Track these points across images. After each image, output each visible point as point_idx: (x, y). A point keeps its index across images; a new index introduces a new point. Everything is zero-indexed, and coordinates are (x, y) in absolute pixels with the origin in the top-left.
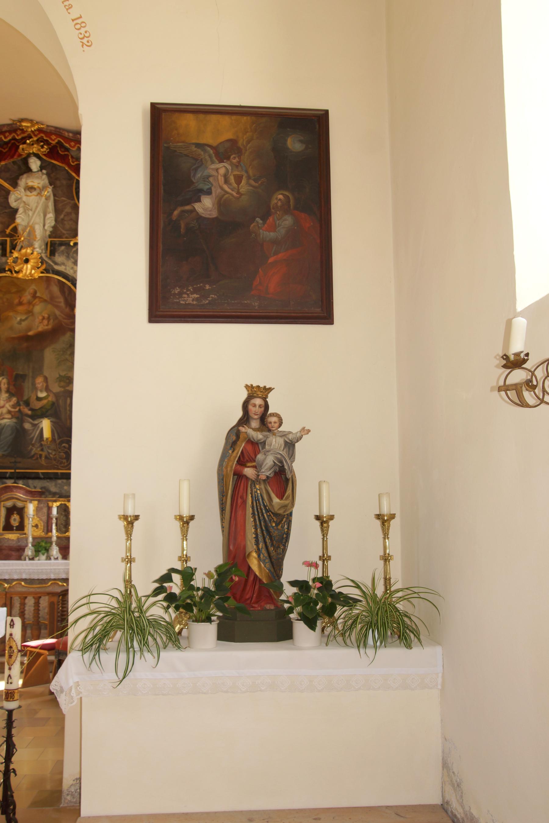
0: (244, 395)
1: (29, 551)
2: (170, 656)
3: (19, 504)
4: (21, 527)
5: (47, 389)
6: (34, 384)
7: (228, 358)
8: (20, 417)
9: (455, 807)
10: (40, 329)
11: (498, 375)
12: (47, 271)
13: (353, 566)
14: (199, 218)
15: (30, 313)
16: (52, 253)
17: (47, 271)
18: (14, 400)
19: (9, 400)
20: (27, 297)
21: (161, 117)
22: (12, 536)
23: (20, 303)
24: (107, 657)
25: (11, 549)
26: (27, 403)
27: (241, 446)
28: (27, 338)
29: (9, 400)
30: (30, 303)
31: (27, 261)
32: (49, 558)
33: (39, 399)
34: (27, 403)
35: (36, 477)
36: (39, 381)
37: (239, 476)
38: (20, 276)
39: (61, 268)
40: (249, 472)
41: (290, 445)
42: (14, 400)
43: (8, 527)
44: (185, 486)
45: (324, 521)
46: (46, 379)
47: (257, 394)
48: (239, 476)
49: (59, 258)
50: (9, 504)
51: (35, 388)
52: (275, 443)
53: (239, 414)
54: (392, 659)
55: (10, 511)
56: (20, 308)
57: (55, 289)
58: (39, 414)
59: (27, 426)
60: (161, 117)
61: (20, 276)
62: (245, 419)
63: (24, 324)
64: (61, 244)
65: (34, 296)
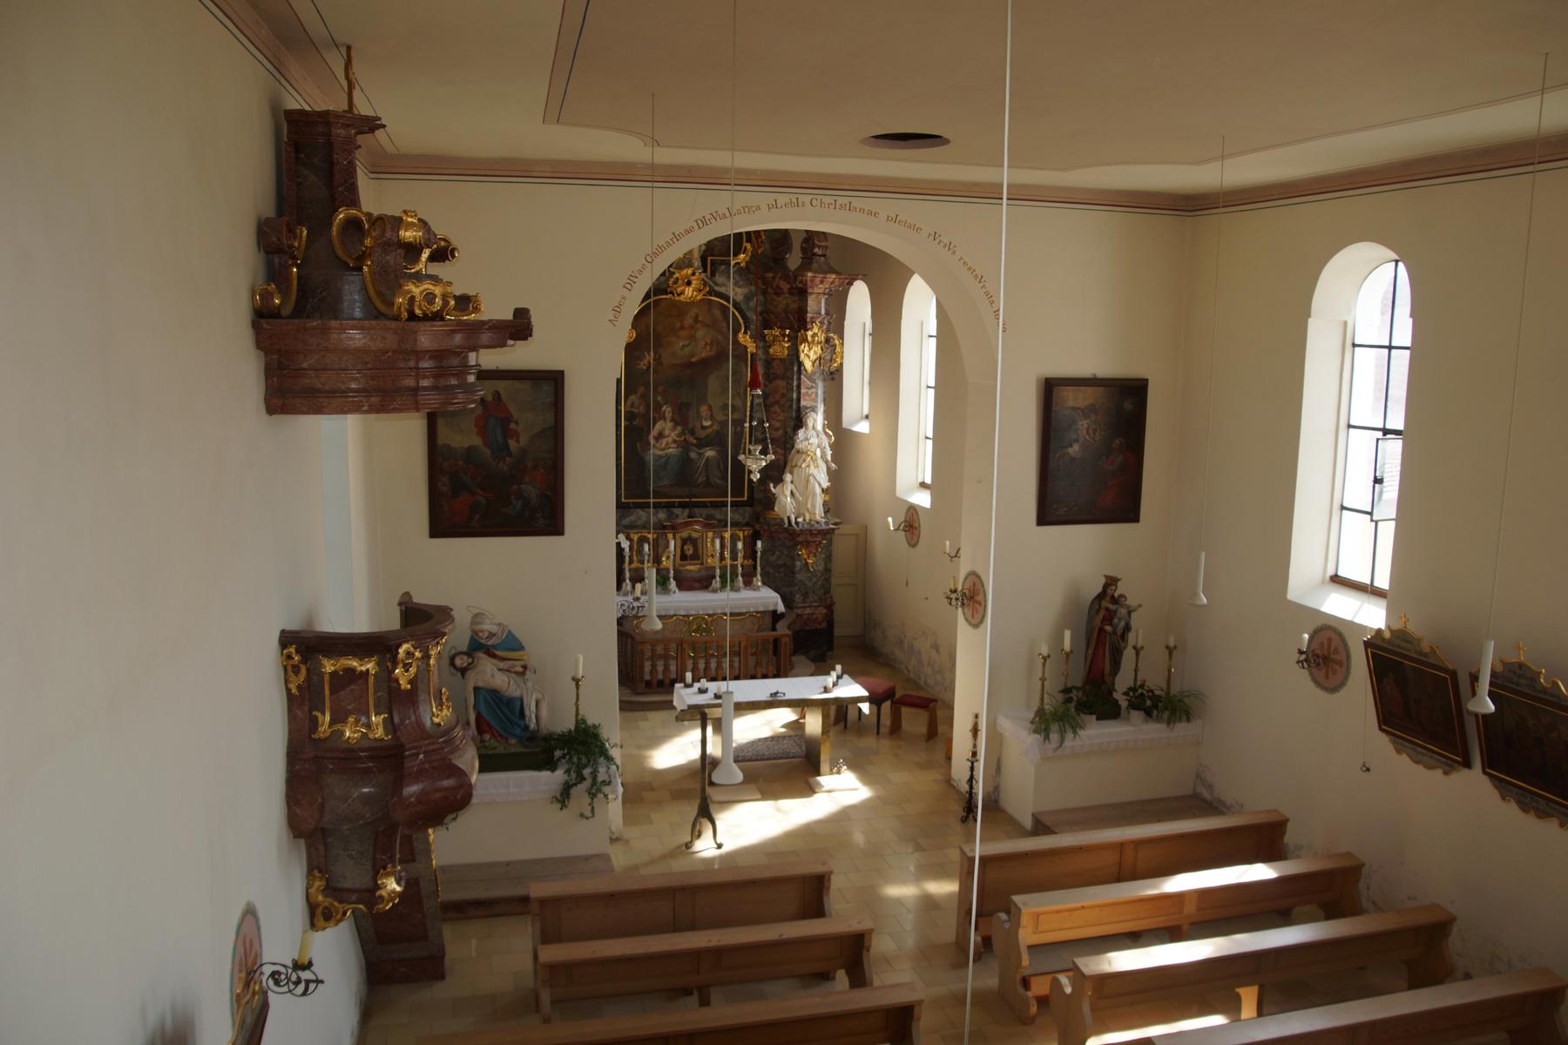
0: (1103, 581)
1: (717, 583)
2: (1081, 733)
3: (695, 535)
4: (696, 556)
5: (712, 418)
6: (698, 412)
7: (1083, 552)
8: (685, 446)
9: (1206, 794)
10: (703, 355)
11: (1296, 656)
12: (709, 293)
13: (1154, 680)
14: (1073, 459)
15: (692, 338)
16: (713, 274)
17: (709, 293)
18: (679, 429)
19: (674, 429)
20: (689, 321)
21: (1050, 388)
22: (692, 567)
23: (682, 328)
24: (1054, 737)
25: (699, 580)
26: (692, 433)
27: (1102, 613)
28: (690, 365)
29: (674, 429)
30: (692, 327)
31: (689, 283)
32: (734, 589)
33: (704, 428)
34: (692, 433)
35: (704, 505)
36: (704, 409)
37: (1101, 630)
38: (682, 298)
39: (722, 290)
40: (1108, 628)
41: (1129, 613)
42: (679, 429)
43: (684, 557)
44: (1067, 634)
45: (1137, 650)
46: (710, 407)
47: (1111, 582)
48: (1101, 630)
49: (719, 279)
50: (685, 534)
51: (699, 417)
52: (1123, 612)
53: (1100, 589)
54: (1182, 729)
55: (684, 542)
56: (682, 333)
57: (717, 313)
58: (703, 443)
59: (693, 455)
60: (1050, 388)
61: (682, 298)
62: (1101, 596)
63: (686, 350)
64: (722, 263)
65: (696, 320)
